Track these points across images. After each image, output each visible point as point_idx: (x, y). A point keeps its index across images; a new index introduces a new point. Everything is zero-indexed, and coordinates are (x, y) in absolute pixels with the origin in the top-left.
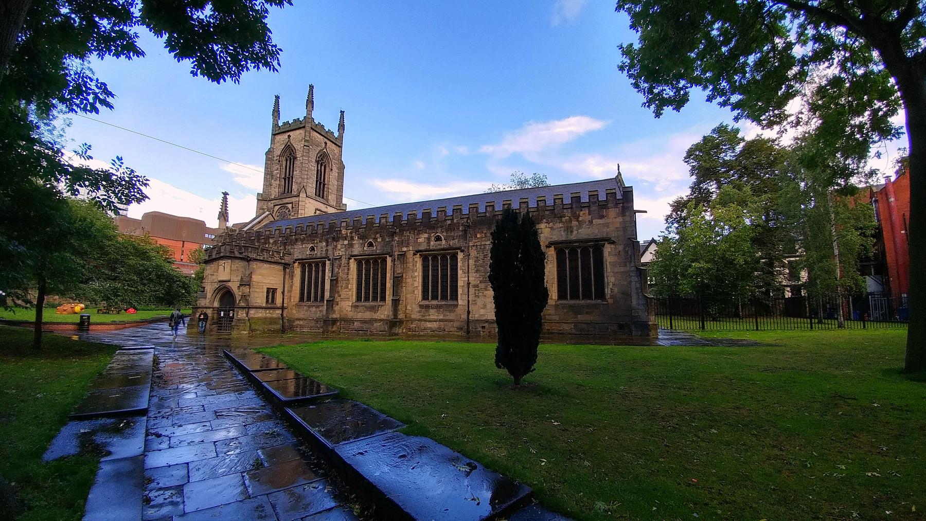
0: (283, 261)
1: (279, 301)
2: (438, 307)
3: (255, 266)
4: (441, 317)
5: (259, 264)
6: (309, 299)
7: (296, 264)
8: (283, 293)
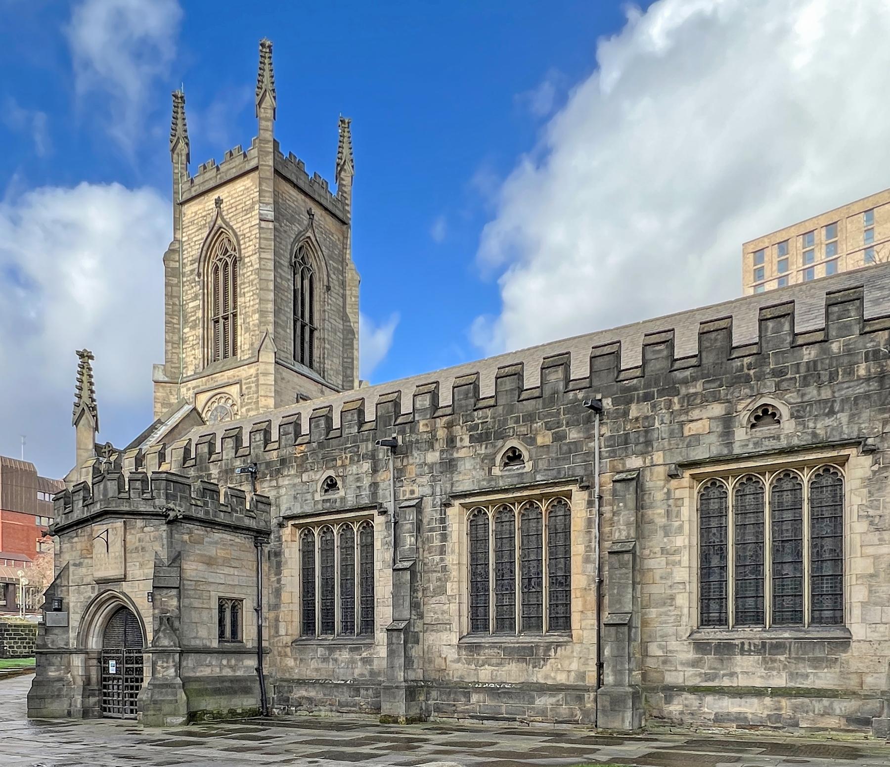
0: (252, 524)
1: (248, 635)
2: (764, 649)
3: (186, 537)
4: (780, 681)
5: (198, 531)
6: (328, 626)
7: (287, 532)
8: (258, 610)
